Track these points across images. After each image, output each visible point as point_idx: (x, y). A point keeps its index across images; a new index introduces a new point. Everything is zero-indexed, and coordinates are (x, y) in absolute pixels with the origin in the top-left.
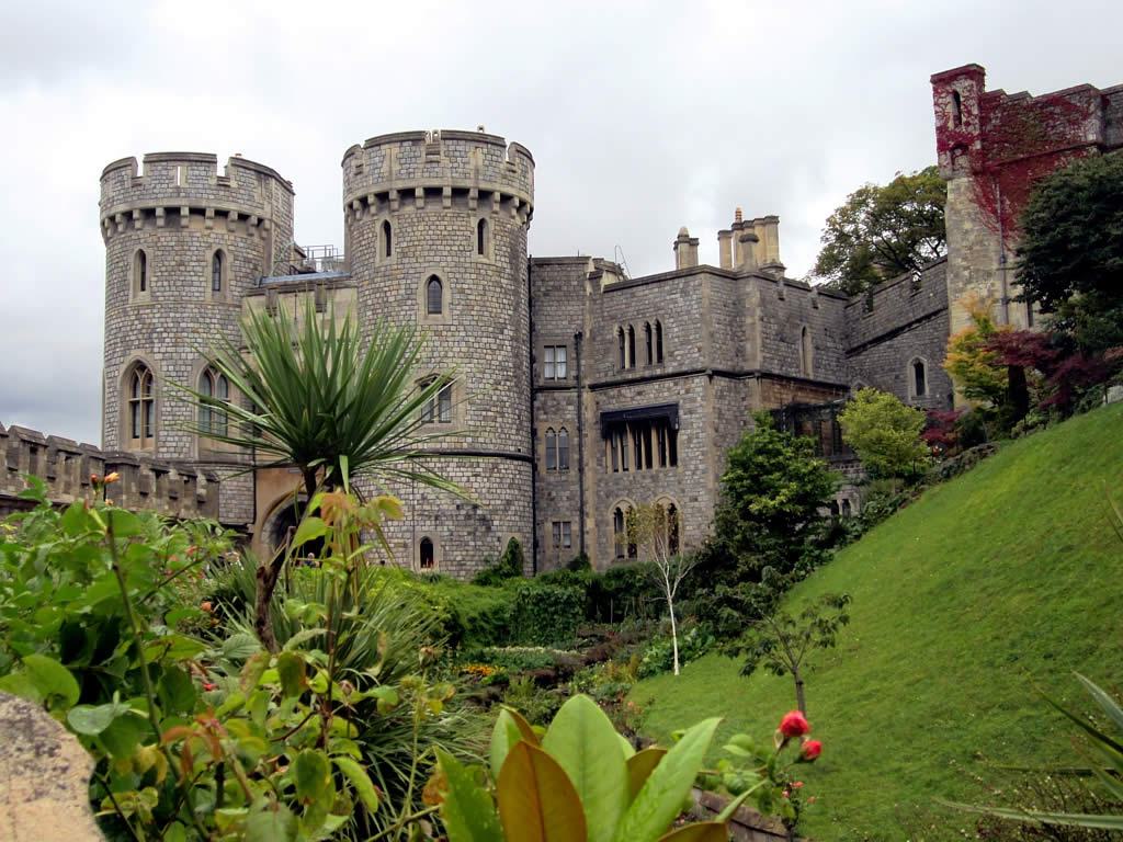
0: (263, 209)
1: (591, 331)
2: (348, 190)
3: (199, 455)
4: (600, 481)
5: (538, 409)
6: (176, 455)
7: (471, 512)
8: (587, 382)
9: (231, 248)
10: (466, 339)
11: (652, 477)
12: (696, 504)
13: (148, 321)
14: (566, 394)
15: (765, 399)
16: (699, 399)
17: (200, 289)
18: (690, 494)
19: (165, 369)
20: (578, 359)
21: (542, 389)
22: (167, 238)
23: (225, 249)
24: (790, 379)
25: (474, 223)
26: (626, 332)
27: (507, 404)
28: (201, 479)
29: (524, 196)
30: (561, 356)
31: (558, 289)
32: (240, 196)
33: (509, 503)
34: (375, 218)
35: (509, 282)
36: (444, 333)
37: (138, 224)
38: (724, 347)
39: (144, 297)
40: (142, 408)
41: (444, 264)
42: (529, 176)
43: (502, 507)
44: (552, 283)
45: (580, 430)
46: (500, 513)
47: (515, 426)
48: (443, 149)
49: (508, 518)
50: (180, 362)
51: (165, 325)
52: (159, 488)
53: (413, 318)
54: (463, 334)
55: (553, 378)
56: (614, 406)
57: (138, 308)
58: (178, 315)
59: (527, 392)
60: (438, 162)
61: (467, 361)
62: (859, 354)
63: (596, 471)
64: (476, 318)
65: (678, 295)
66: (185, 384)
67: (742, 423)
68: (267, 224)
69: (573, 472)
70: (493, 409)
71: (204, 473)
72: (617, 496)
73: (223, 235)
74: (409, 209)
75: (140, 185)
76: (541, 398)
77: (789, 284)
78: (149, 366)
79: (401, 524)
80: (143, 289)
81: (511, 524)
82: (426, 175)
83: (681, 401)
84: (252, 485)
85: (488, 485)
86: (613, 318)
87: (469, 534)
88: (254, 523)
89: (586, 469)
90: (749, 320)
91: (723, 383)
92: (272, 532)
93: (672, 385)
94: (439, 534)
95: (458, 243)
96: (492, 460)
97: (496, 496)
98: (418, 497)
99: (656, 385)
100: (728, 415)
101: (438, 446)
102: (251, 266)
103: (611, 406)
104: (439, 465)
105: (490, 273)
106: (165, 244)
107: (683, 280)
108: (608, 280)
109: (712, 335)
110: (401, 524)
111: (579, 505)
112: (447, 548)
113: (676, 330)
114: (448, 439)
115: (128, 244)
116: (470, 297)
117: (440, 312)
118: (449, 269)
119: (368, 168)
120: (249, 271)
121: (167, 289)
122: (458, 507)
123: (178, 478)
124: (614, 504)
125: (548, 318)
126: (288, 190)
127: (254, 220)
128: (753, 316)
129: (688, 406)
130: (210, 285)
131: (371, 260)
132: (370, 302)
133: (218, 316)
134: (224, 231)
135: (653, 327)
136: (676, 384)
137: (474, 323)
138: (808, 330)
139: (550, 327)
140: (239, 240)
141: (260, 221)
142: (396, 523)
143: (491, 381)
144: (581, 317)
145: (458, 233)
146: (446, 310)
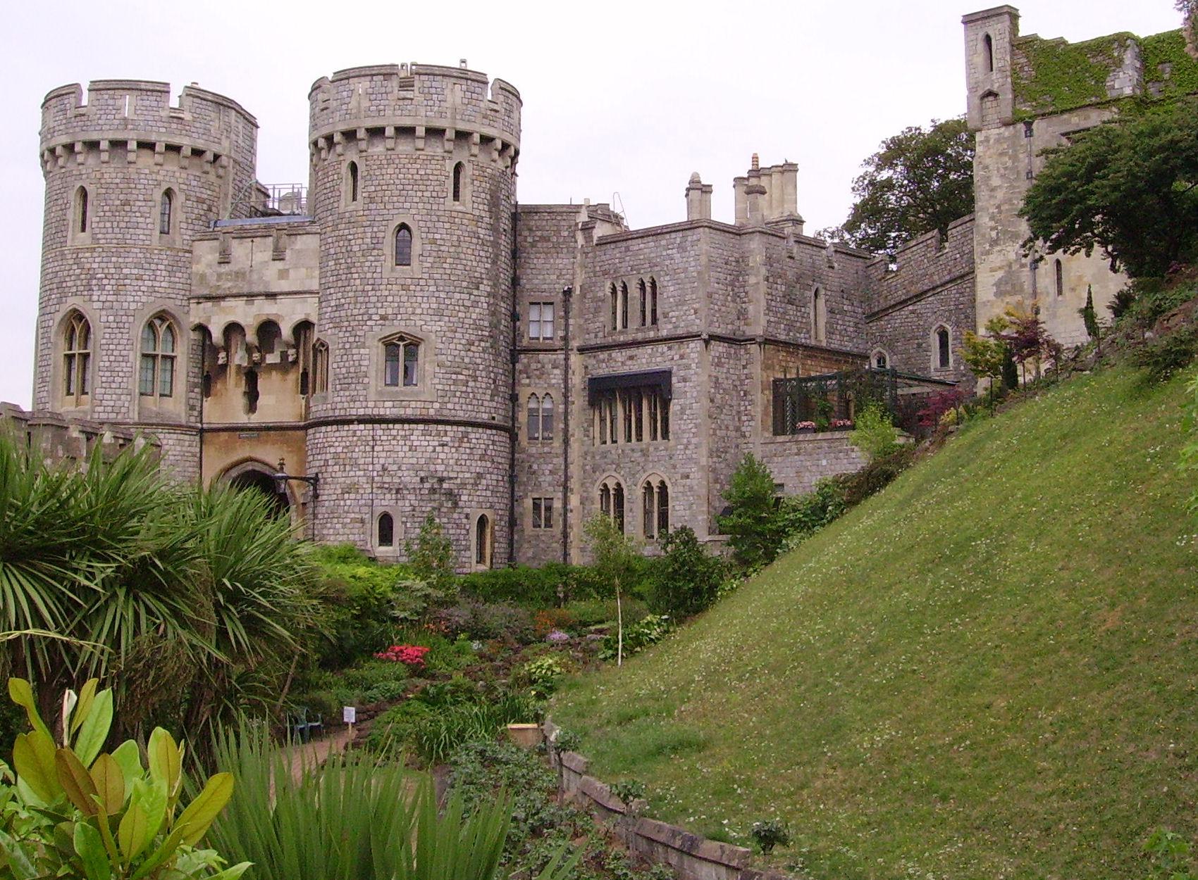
0: (220, 143)
2: (314, 127)
4: (586, 454)
5: (520, 372)
6: (113, 415)
7: (436, 486)
8: (575, 344)
9: (182, 186)
10: (436, 294)
11: (642, 451)
13: (88, 266)
14: (552, 357)
15: (767, 367)
16: (694, 366)
17: (147, 232)
18: (681, 471)
19: (104, 319)
20: (566, 317)
21: (526, 351)
22: (112, 172)
23: (176, 189)
24: (797, 346)
25: (450, 167)
26: (619, 289)
27: (481, 367)
28: (140, 442)
29: (509, 138)
30: (548, 314)
32: (193, 129)
33: (480, 476)
34: (342, 158)
35: (487, 232)
36: (412, 287)
38: (723, 309)
39: (84, 239)
40: (77, 362)
41: (414, 211)
42: (515, 115)
43: (472, 481)
44: (539, 233)
45: (566, 396)
46: (469, 487)
47: (489, 392)
48: (417, 84)
49: (478, 493)
51: (106, 271)
53: (379, 270)
55: (538, 339)
56: (603, 371)
57: (77, 251)
58: (121, 260)
59: (505, 354)
60: (412, 99)
61: (436, 318)
62: (879, 319)
63: (583, 443)
64: (448, 271)
65: (675, 251)
66: (126, 336)
67: (742, 393)
68: (224, 161)
69: (557, 444)
74: (378, 148)
76: (524, 359)
77: (801, 241)
78: (87, 317)
79: (359, 497)
80: (83, 230)
81: (481, 499)
82: (399, 112)
84: (198, 450)
85: (456, 456)
86: (605, 273)
90: (752, 280)
91: (721, 349)
93: (665, 349)
94: (400, 510)
95: (431, 188)
96: (462, 429)
97: (464, 468)
98: (378, 467)
99: (649, 349)
100: (727, 384)
102: (205, 207)
104: (402, 433)
105: (465, 221)
106: (109, 181)
107: (680, 234)
108: (601, 230)
109: (710, 295)
110: (359, 497)
112: (408, 525)
113: (672, 288)
114: (413, 404)
116: (442, 248)
117: (409, 265)
118: (420, 218)
120: (202, 212)
121: (110, 230)
122: (422, 479)
124: (601, 478)
125: (534, 271)
126: (250, 122)
129: (682, 373)
132: (332, 251)
133: (166, 262)
134: (176, 169)
135: (648, 285)
136: (670, 348)
137: (446, 277)
138: (822, 292)
140: (192, 177)
141: (217, 157)
142: (352, 496)
143: (464, 342)
145: (431, 177)
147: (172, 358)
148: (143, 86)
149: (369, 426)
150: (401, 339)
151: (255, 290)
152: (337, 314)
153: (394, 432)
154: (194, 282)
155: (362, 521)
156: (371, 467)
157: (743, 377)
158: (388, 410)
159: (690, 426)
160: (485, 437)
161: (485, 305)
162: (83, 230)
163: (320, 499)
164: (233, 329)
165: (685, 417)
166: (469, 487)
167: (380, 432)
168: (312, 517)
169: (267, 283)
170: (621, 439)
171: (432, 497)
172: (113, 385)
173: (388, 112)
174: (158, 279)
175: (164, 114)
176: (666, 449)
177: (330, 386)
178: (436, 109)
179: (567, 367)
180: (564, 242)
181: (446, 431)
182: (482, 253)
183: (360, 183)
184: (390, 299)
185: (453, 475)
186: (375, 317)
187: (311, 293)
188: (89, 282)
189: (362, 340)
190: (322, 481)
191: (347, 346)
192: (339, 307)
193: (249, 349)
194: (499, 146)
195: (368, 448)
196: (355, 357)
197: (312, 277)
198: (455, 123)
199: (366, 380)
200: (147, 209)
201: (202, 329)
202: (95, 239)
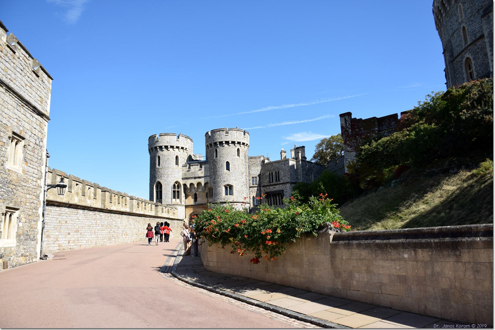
8: (262, 185)
13: (161, 172)
19: (165, 183)
41: (230, 159)
44: (253, 162)
50: (168, 182)
52: (166, 211)
56: (268, 190)
68: (187, 149)
70: (241, 192)
86: (268, 170)
90: (299, 171)
99: (278, 186)
108: (266, 161)
109: (291, 174)
114: (231, 199)
127: (185, 149)
128: (300, 170)
129: (286, 191)
132: (212, 168)
133: (177, 171)
135: (277, 173)
136: (283, 186)
138: (313, 173)
141: (186, 149)
147: (178, 192)
148: (171, 134)
150: (228, 185)
151: (196, 176)
161: (245, 178)
164: (191, 184)
169: (198, 175)
177: (213, 196)
182: (244, 167)
183: (218, 153)
184: (225, 177)
186: (222, 181)
187: (208, 176)
194: (246, 145)
200: (173, 160)
201: (185, 185)
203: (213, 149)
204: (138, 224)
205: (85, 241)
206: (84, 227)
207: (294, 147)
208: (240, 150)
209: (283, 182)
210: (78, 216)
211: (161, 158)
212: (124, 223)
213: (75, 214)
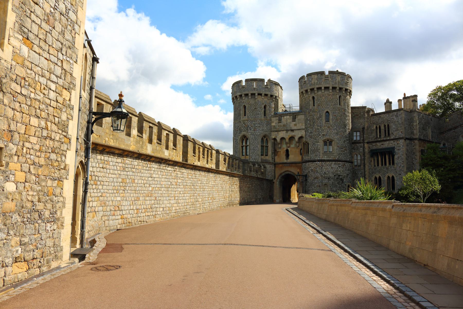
1: (367, 127)
3: (261, 160)
4: (370, 169)
6: (254, 161)
7: (338, 177)
8: (366, 141)
11: (386, 168)
12: (401, 176)
15: (420, 146)
16: (401, 146)
18: (398, 173)
19: (251, 137)
20: (363, 135)
22: (252, 101)
23: (267, 105)
25: (338, 96)
26: (378, 127)
27: (347, 147)
28: (262, 167)
31: (357, 115)
34: (310, 95)
37: (244, 98)
39: (246, 118)
41: (330, 108)
45: (364, 154)
46: (346, 177)
49: (348, 179)
50: (256, 135)
51: (251, 125)
52: (254, 169)
53: (322, 123)
54: (335, 127)
56: (374, 148)
57: (244, 121)
58: (255, 122)
61: (337, 135)
63: (369, 166)
64: (339, 123)
65: (394, 117)
66: (257, 141)
67: (413, 153)
69: (362, 166)
70: (344, 148)
71: (263, 165)
72: (375, 173)
73: (266, 101)
74: (320, 93)
75: (244, 87)
80: (245, 115)
83: (396, 147)
84: (274, 169)
85: (342, 170)
86: (374, 123)
87: (338, 183)
88: (275, 179)
89: (366, 165)
91: (408, 142)
92: (279, 182)
93: (393, 142)
95: (334, 102)
96: (343, 163)
97: (345, 173)
98: (323, 173)
99: (388, 142)
101: (329, 159)
103: (374, 148)
105: (342, 110)
107: (396, 112)
108: (371, 113)
109: (405, 128)
111: (364, 175)
112: (332, 187)
114: (332, 157)
115: (241, 103)
116: (337, 117)
117: (329, 121)
119: (308, 82)
121: (252, 115)
123: (257, 167)
125: (355, 123)
128: (416, 122)
130: (263, 114)
131: (309, 107)
132: (308, 119)
133: (265, 123)
134: (267, 100)
136: (394, 142)
137: (339, 124)
138: (430, 127)
139: (355, 126)
142: (317, 180)
143: (343, 141)
144: (364, 123)
146: (331, 121)
147: (267, 147)
149: (321, 162)
150: (328, 140)
151: (288, 129)
152: (311, 134)
153: (327, 164)
154: (272, 128)
155: (320, 186)
156: (321, 173)
157: (413, 149)
158: (325, 158)
159: (401, 162)
160: (349, 165)
162: (245, 115)
163: (307, 180)
164: (283, 139)
165: (399, 159)
166: (346, 177)
167: (324, 164)
168: (305, 185)
169: (291, 128)
170: (380, 165)
171: (337, 180)
172: (254, 153)
173: (323, 83)
174: (264, 127)
175: (264, 86)
176: (394, 168)
177: (309, 153)
178: (334, 82)
179: (364, 147)
180: (362, 116)
181: (340, 163)
183: (315, 102)
184: (325, 130)
185: (342, 174)
188: (247, 128)
189: (318, 141)
190: (308, 176)
191: (314, 142)
192: (311, 133)
193: (286, 143)
195: (320, 168)
196: (316, 145)
197: (303, 126)
198: (339, 86)
199: (319, 151)
201: (275, 139)
202: (248, 117)
203: (309, 97)
204: (226, 184)
205: (161, 209)
206: (160, 189)
207: (403, 97)
208: (343, 98)
209: (395, 138)
210: (152, 172)
211: (247, 107)
212: (210, 183)
213: (147, 168)
